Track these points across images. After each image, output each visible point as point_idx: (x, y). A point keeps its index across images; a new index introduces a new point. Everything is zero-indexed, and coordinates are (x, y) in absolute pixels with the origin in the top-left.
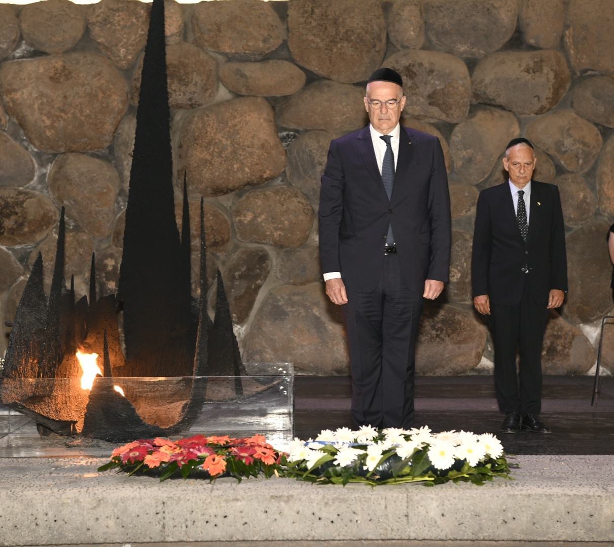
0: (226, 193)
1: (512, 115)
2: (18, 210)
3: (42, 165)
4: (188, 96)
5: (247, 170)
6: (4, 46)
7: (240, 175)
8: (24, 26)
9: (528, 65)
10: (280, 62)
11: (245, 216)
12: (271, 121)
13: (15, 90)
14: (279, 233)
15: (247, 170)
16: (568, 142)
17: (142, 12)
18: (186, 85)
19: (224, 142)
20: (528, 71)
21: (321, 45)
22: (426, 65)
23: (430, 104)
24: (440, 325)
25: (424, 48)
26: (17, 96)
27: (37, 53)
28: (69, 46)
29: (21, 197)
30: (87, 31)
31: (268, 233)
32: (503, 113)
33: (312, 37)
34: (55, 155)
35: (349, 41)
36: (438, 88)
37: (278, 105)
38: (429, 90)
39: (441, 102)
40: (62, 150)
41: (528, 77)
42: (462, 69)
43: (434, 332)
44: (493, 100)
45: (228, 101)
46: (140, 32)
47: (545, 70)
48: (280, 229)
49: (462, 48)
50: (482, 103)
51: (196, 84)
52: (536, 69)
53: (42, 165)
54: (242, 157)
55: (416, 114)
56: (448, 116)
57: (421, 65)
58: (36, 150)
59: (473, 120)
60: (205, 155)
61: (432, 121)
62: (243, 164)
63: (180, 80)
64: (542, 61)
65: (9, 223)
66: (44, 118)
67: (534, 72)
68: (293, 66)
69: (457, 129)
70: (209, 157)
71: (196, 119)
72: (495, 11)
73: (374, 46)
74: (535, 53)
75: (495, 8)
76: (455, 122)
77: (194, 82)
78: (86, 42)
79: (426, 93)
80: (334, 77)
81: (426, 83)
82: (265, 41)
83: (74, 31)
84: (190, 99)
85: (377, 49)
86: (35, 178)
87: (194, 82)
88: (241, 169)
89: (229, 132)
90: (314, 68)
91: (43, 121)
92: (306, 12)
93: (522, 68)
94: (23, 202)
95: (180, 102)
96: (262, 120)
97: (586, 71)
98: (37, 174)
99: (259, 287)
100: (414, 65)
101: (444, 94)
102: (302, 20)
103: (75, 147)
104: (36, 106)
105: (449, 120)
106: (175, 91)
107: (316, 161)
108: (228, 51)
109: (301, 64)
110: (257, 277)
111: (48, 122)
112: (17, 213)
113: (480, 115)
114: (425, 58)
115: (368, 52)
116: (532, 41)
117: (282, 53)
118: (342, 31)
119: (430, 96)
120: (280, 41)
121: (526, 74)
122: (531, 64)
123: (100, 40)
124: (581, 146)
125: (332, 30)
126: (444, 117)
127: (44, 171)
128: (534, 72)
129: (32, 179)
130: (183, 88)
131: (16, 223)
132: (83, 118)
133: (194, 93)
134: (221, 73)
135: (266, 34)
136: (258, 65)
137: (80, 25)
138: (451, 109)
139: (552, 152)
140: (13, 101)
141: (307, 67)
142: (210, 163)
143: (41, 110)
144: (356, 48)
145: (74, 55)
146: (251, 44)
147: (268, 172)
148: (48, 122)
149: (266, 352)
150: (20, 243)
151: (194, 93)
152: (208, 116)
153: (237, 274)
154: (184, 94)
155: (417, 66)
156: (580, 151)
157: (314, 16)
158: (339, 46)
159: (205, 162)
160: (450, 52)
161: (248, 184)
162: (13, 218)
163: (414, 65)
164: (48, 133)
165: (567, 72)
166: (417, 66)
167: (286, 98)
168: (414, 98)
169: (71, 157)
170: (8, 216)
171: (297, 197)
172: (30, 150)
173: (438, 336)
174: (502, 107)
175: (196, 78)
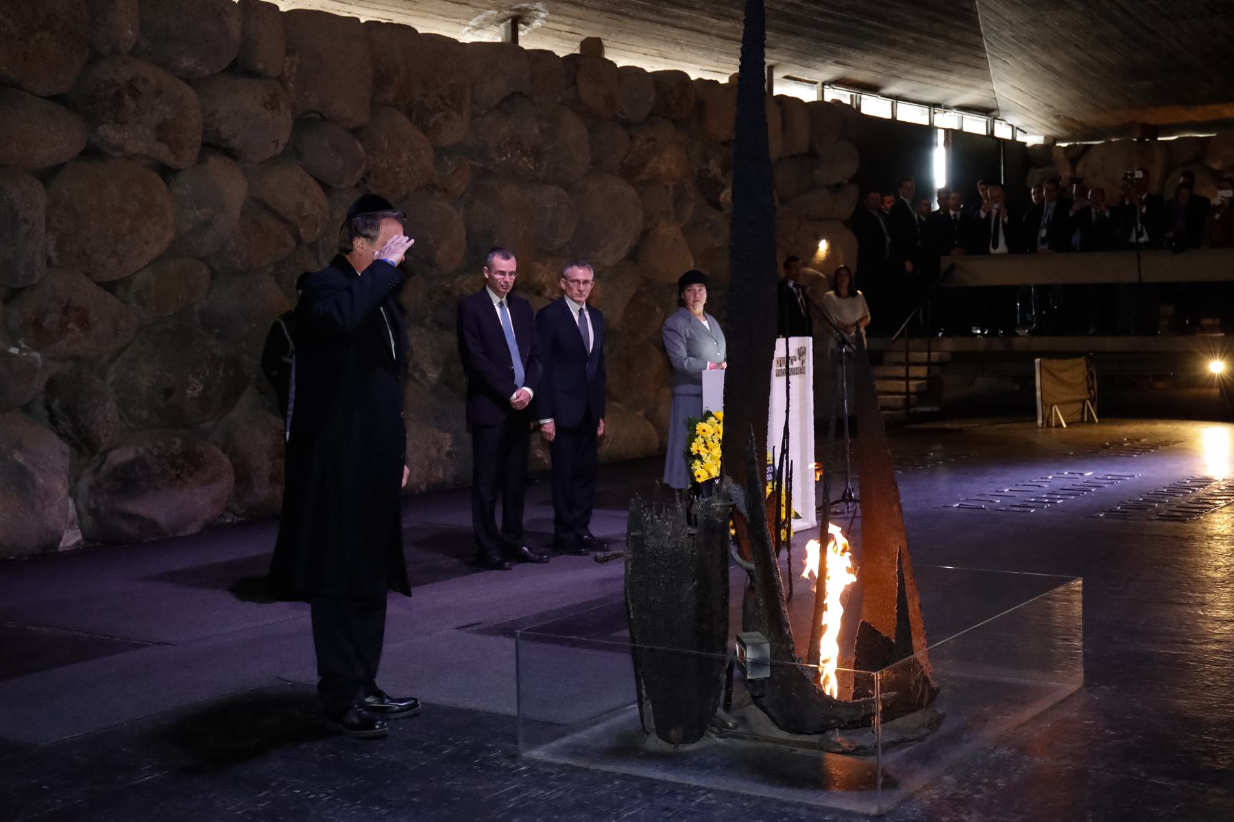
20: (265, 106)
23: (158, 139)
24: (180, 461)
36: (168, 117)
43: (174, 471)
49: (187, 63)
50: (214, 146)
57: (145, 81)
81: (152, 109)
173: (178, 476)
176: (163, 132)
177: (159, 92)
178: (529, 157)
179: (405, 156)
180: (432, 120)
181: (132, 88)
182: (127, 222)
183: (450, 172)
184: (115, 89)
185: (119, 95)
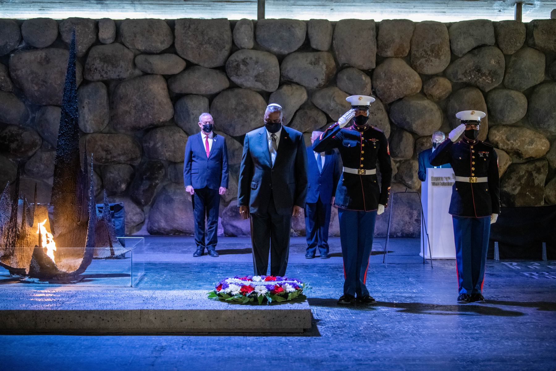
0: (139, 130)
1: (303, 89)
2: (19, 138)
3: (33, 112)
4: (117, 74)
5: (150, 117)
6: (12, 44)
7: (146, 120)
8: (23, 32)
9: (311, 60)
10: (170, 55)
11: (149, 143)
12: (165, 89)
13: (17, 70)
14: (169, 153)
15: (150, 117)
16: (332, 104)
17: (91, 25)
18: (116, 67)
19: (138, 101)
20: (311, 64)
21: (194, 46)
22: (254, 58)
23: (256, 81)
25: (254, 49)
26: (19, 73)
27: (30, 47)
28: (50, 43)
29: (21, 131)
30: (59, 35)
31: (163, 153)
32: (298, 86)
33: (189, 41)
34: (40, 107)
35: (210, 44)
37: (169, 79)
38: (255, 73)
39: (262, 80)
40: (44, 104)
41: (311, 67)
42: (274, 61)
44: (292, 79)
45: (139, 76)
46: (90, 36)
47: (321, 64)
48: (170, 151)
49: (275, 49)
50: (285, 81)
51: (122, 67)
52: (315, 63)
53: (33, 112)
54: (147, 110)
55: (249, 86)
56: (266, 87)
57: (251, 58)
58: (30, 104)
59: (280, 90)
60: (126, 108)
61: (258, 90)
62: (148, 114)
63: (113, 65)
64: (319, 58)
65: (13, 146)
66: (34, 85)
67: (315, 65)
68: (178, 57)
69: (272, 95)
70: (128, 109)
71: (121, 87)
72: (293, 29)
73: (224, 47)
74: (315, 53)
75: (293, 27)
76: (270, 91)
77: (120, 66)
78: (59, 42)
79: (254, 74)
80: (201, 64)
82: (162, 43)
83: (52, 36)
84: (118, 76)
85: (226, 48)
86: (29, 120)
87: (120, 66)
88: (147, 116)
89: (140, 95)
90: (191, 59)
91: (34, 87)
92: (185, 27)
93: (308, 62)
94: (22, 133)
95: (112, 77)
96: (159, 89)
97: (345, 64)
98: (30, 117)
99: (157, 184)
100: (247, 59)
101: (264, 75)
102: (184, 31)
103: (51, 103)
104: (29, 79)
105: (267, 90)
106: (109, 71)
107: (190, 113)
108: (140, 48)
109: (183, 56)
110: (156, 178)
111: (36, 88)
112: (17, 140)
113: (285, 88)
114: (254, 54)
115: (221, 50)
116: (314, 47)
117: (172, 50)
118: (206, 38)
119: (256, 77)
120: (171, 43)
121: (310, 65)
122: (313, 60)
123: (67, 41)
124: (340, 107)
125: (200, 38)
126: (264, 88)
127: (34, 115)
128: (315, 65)
129: (27, 121)
130: (114, 69)
131: (17, 145)
132: (56, 86)
133: (121, 72)
134: (136, 61)
135: (162, 39)
136: (158, 56)
137: (55, 32)
138: (268, 84)
139: (325, 110)
140: (16, 75)
141: (185, 58)
142: (129, 113)
143: (32, 81)
144: (214, 48)
145: (52, 50)
146: (153, 44)
147: (163, 118)
148: (36, 88)
149: (161, 222)
150: (20, 157)
151: (121, 72)
152: (128, 86)
153: (144, 177)
154: (115, 72)
155: (249, 59)
156: (340, 110)
157: (190, 29)
158: (204, 46)
159: (126, 112)
160: (269, 51)
161: (151, 125)
162: (16, 143)
163: (247, 59)
164: (36, 94)
165: (333, 64)
166: (249, 59)
167: (174, 76)
168: (247, 77)
169: (50, 109)
170: (13, 142)
171: (179, 133)
172: (26, 103)
174: (297, 84)
175: (122, 63)
176: (257, 78)
177: (257, 62)
178: (486, 76)
179: (394, 81)
180: (418, 63)
181: (244, 62)
182: (237, 114)
183: (431, 86)
184: (236, 63)
185: (238, 65)
